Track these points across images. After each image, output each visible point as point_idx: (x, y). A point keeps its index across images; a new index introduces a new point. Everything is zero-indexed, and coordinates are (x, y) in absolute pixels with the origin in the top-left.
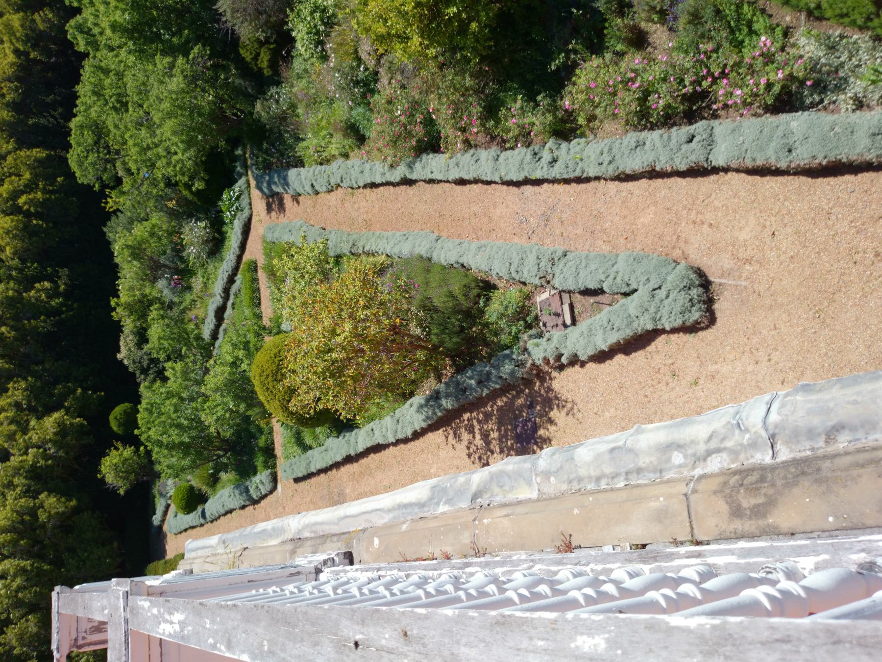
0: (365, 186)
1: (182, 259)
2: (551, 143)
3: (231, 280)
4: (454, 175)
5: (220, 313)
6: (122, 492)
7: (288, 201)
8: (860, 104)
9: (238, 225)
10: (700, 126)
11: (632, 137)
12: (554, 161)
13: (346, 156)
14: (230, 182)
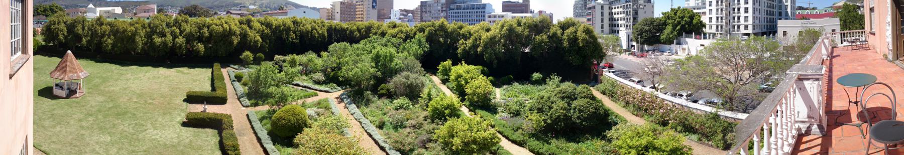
5: (298, 85)
6: (240, 57)
9: (327, 89)
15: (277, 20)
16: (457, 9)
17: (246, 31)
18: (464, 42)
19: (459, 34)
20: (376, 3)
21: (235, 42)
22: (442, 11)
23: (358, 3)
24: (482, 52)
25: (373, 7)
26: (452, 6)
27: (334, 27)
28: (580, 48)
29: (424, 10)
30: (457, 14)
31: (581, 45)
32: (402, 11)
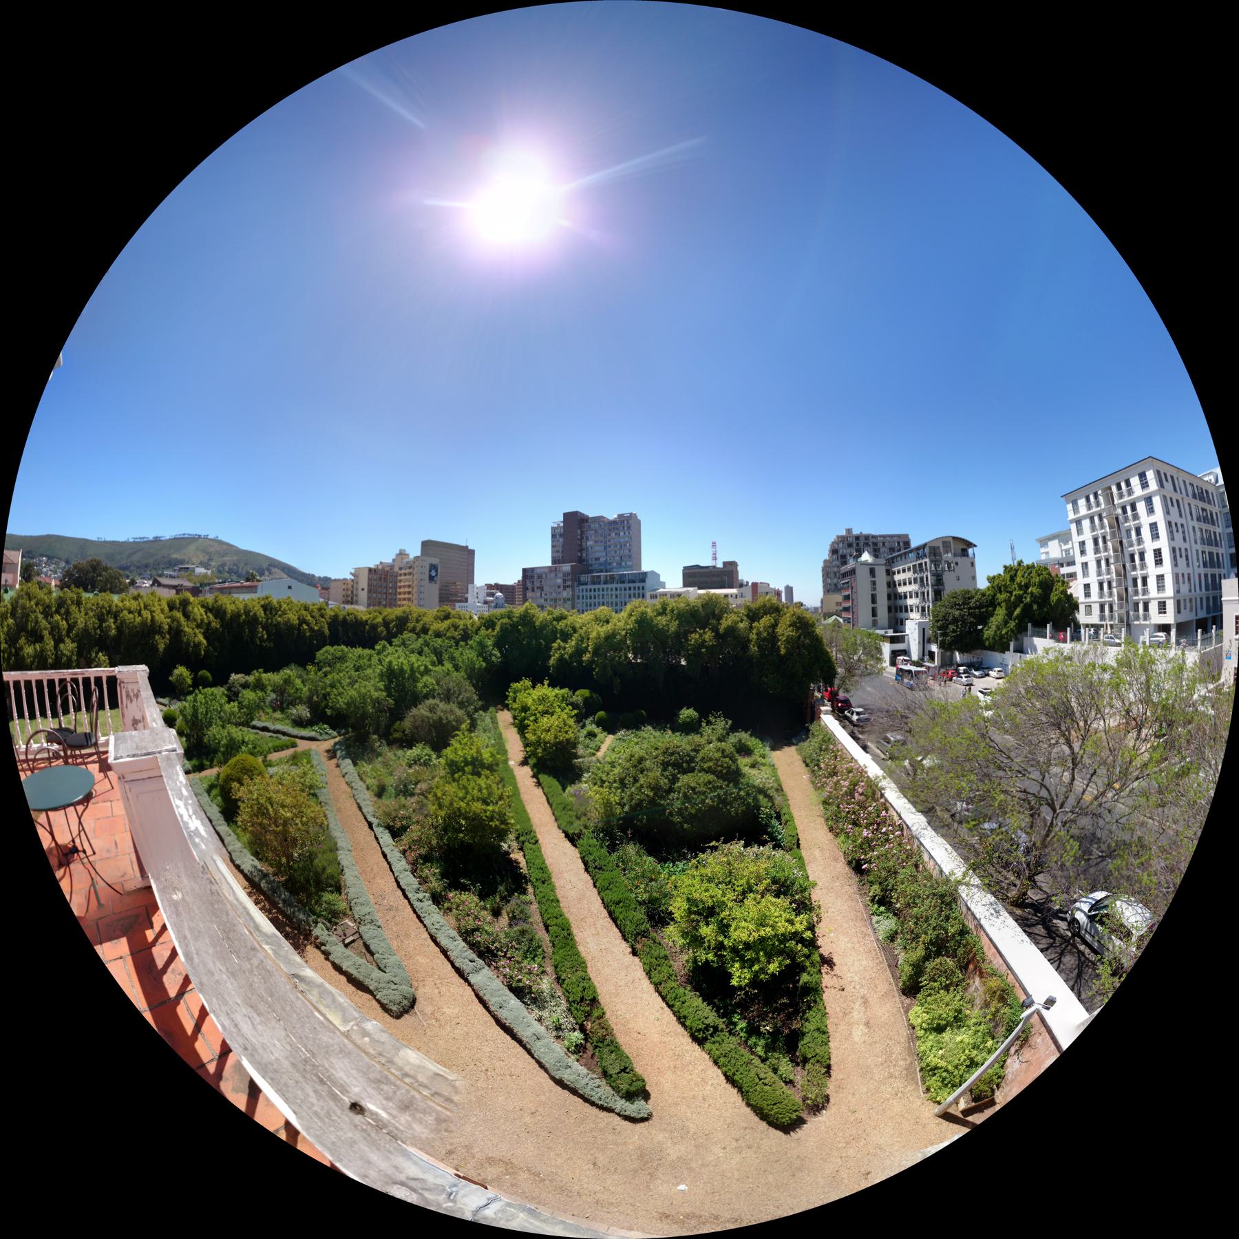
0: (358, 804)
1: (288, 706)
2: (428, 895)
3: (284, 734)
4: (387, 850)
7: (334, 761)
8: (540, 1020)
10: (481, 962)
11: (454, 933)
12: (421, 901)
13: (368, 788)
14: (333, 728)
15: (240, 601)
16: (593, 583)
17: (179, 625)
18: (562, 644)
19: (554, 631)
20: (437, 571)
21: (161, 647)
22: (565, 588)
23: (403, 571)
24: (591, 662)
25: (431, 578)
26: (584, 578)
27: (341, 617)
28: (781, 658)
29: (529, 585)
30: (592, 593)
31: (783, 651)
32: (489, 586)
